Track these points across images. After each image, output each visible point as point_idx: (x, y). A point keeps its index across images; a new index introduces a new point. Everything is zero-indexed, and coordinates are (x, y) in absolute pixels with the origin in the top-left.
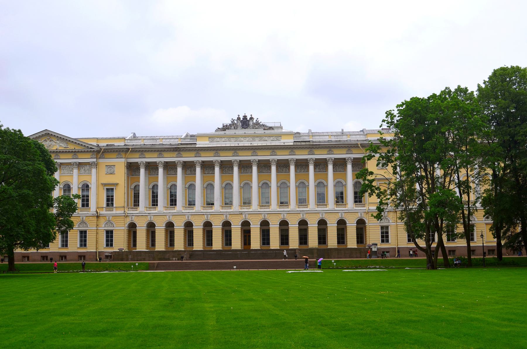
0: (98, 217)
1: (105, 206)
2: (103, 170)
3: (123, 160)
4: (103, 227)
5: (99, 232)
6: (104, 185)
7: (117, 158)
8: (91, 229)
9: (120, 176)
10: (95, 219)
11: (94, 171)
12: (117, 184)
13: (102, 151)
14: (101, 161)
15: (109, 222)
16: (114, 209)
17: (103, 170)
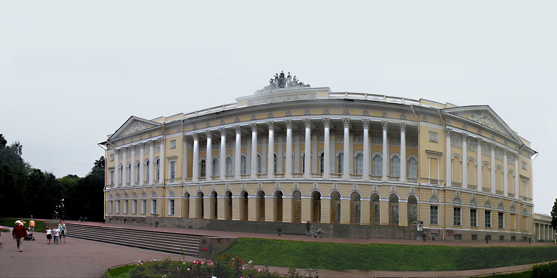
0: (164, 188)
1: (169, 178)
2: (169, 145)
3: (181, 134)
4: (168, 196)
5: (166, 202)
6: (169, 158)
7: (177, 133)
8: (159, 197)
9: (180, 150)
10: (162, 189)
11: (162, 146)
12: (176, 157)
13: (166, 128)
14: (167, 137)
15: (171, 193)
16: (175, 180)
17: (169, 145)
